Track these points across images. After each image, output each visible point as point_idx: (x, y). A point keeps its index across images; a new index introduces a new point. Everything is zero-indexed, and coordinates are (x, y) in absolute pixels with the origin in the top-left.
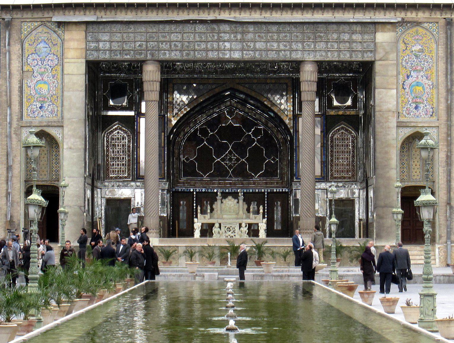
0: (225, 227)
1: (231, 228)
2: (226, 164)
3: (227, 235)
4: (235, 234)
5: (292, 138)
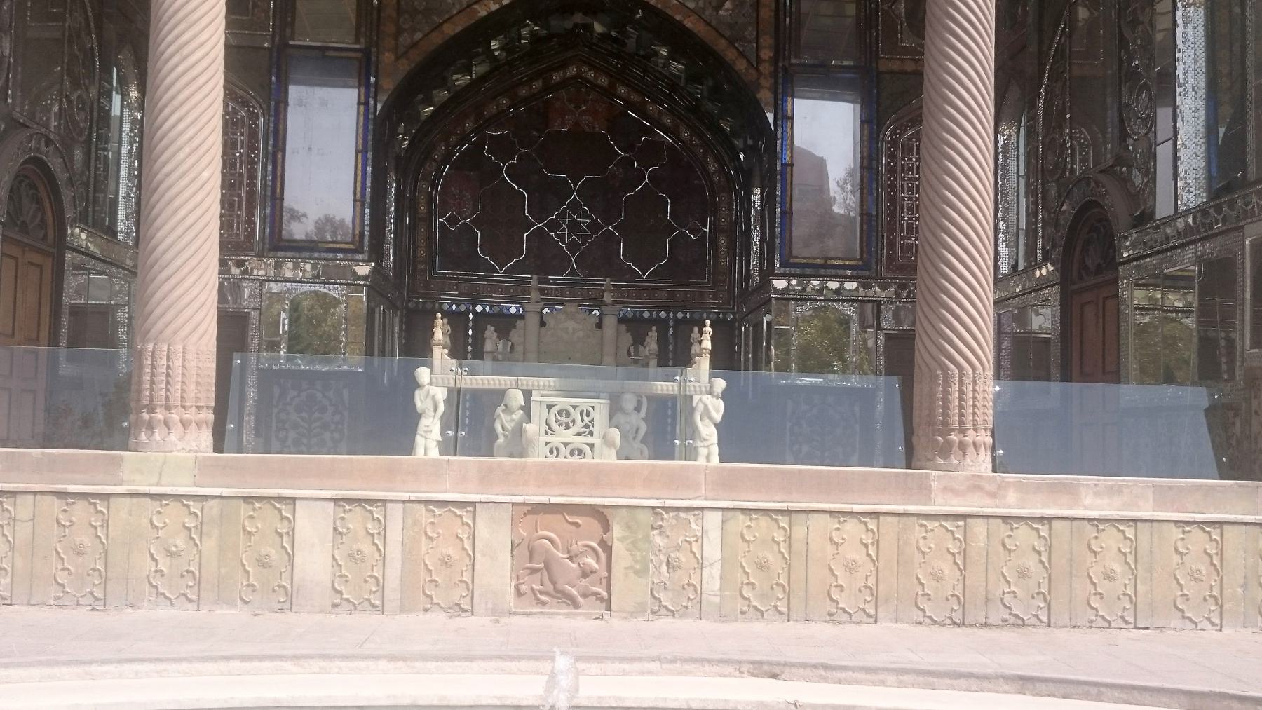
0: (550, 407)
1: (575, 414)
2: (562, 237)
3: (556, 441)
4: (590, 440)
5: (772, 138)
